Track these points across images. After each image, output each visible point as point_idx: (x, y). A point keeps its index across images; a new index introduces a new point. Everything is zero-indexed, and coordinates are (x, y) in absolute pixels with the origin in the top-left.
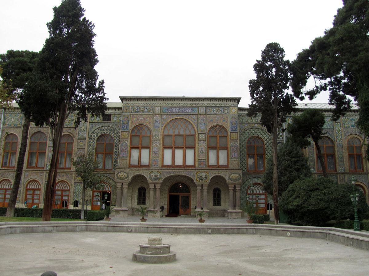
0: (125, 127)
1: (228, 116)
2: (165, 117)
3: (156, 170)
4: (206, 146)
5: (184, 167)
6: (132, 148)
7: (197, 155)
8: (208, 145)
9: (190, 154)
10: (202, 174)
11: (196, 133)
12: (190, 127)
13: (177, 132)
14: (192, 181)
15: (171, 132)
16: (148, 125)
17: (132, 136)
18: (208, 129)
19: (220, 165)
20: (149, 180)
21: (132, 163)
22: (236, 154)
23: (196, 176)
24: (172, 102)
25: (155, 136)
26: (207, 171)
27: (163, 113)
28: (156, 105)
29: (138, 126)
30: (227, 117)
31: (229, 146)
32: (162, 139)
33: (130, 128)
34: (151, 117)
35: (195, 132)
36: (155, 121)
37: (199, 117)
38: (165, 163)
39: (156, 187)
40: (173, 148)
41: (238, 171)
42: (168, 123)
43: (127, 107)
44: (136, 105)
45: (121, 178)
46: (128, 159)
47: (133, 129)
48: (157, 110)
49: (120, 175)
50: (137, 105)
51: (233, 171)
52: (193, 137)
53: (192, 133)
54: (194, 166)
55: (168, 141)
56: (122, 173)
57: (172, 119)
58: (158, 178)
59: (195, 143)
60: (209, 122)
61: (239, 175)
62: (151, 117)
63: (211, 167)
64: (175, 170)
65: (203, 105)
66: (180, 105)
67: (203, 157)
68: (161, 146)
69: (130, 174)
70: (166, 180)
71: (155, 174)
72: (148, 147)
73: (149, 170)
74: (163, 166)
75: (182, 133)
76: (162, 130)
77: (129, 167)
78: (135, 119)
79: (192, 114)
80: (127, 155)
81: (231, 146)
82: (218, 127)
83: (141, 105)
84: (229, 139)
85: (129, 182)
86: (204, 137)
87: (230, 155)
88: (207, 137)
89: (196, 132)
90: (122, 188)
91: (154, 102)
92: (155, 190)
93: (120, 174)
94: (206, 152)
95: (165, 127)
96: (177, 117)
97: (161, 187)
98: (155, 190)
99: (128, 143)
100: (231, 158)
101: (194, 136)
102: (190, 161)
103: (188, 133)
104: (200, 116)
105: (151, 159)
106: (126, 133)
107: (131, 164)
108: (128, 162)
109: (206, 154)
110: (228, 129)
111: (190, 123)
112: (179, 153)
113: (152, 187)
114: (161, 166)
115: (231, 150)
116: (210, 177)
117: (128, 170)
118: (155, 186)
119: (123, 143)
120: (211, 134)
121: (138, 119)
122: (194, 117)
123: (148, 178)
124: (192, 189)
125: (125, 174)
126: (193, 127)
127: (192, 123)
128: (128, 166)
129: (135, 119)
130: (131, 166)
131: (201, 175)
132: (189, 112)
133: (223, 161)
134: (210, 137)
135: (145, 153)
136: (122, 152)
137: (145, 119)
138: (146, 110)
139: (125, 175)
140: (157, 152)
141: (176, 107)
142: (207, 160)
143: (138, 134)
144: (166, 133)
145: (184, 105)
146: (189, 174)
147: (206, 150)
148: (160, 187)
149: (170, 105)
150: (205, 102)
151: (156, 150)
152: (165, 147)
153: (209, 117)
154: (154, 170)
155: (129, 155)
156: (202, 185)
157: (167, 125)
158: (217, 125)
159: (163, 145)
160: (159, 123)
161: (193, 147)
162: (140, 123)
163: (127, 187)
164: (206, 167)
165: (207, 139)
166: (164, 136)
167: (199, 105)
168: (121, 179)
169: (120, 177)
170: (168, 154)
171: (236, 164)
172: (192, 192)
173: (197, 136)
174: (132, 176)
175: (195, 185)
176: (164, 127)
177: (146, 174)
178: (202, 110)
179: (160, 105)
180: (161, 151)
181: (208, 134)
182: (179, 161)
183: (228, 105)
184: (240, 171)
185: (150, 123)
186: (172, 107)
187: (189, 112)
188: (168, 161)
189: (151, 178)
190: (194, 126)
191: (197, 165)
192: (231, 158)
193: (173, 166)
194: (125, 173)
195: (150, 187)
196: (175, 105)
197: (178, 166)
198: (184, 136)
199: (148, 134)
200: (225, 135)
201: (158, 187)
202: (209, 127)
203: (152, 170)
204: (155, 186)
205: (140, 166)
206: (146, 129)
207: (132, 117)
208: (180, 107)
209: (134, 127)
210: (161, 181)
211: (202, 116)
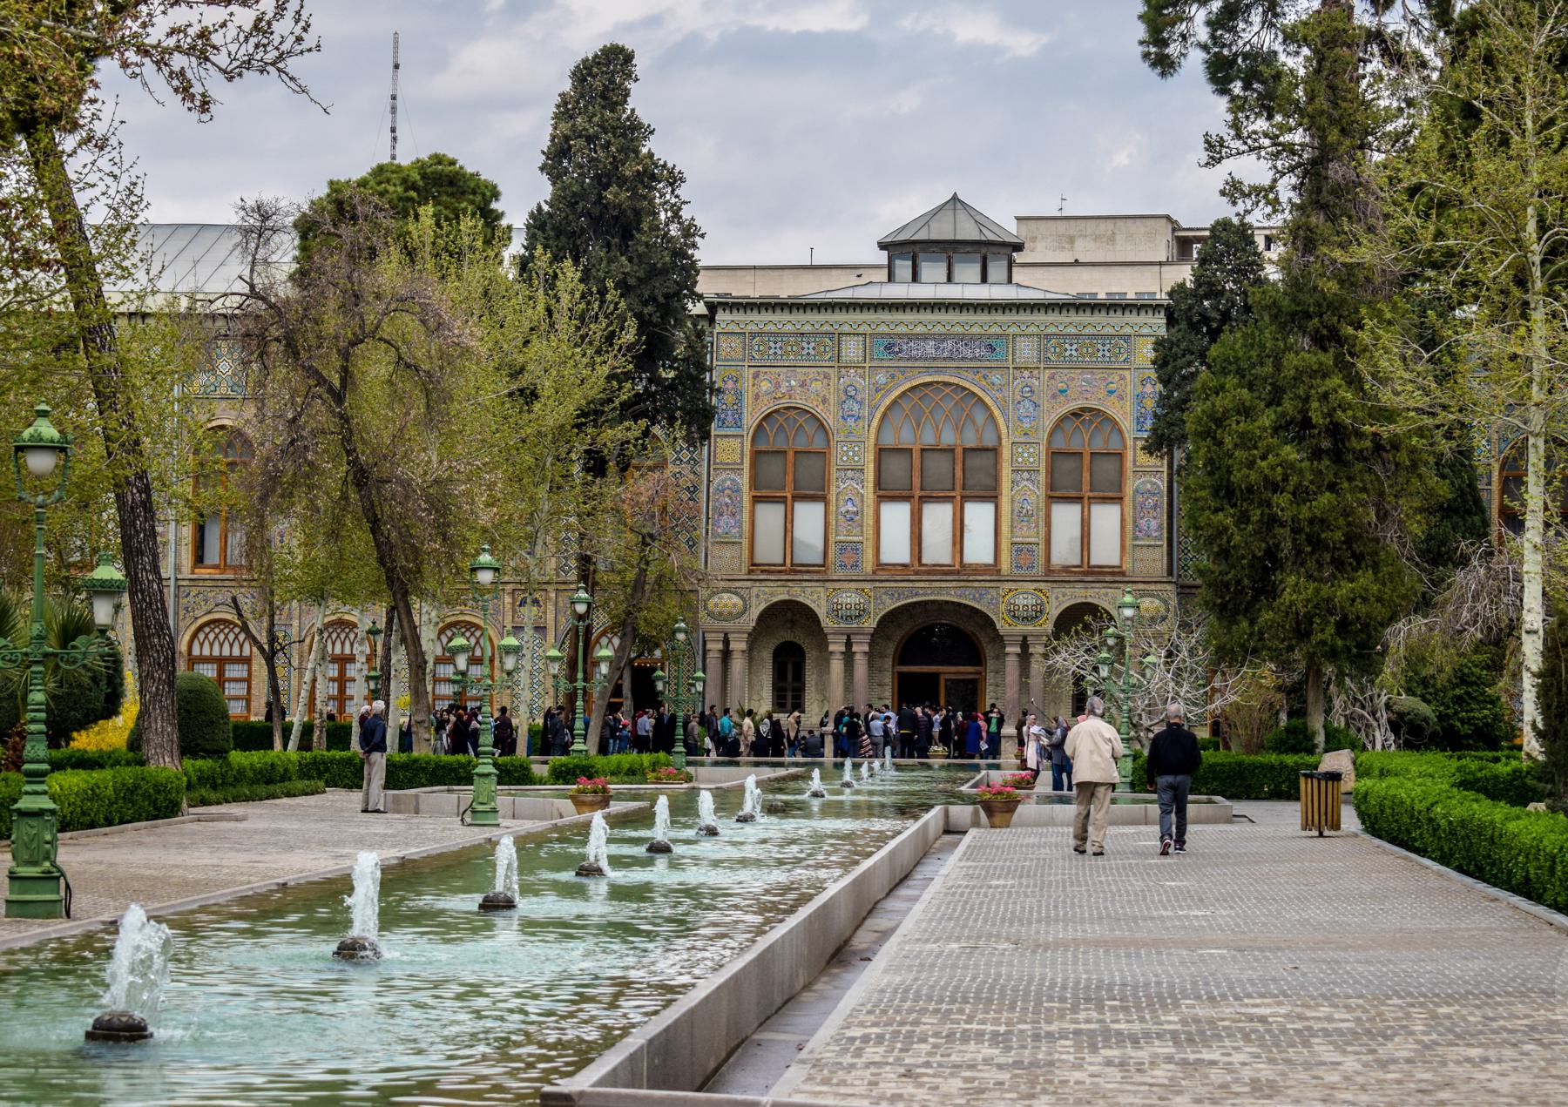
0: (730, 418)
1: (1126, 373)
2: (881, 378)
3: (854, 585)
4: (1042, 493)
5: (958, 573)
6: (757, 500)
7: (1005, 529)
8: (1051, 486)
9: (979, 516)
10: (1024, 601)
11: (1004, 442)
12: (980, 417)
13: (928, 439)
14: (988, 623)
15: (906, 438)
16: (819, 410)
17: (757, 455)
18: (1048, 422)
19: (1094, 562)
20: (827, 623)
21: (761, 557)
22: (1154, 524)
23: (1003, 607)
24: (910, 317)
25: (841, 455)
26: (1042, 586)
27: (875, 364)
28: (846, 329)
29: (776, 411)
30: (1122, 378)
31: (1129, 491)
32: (871, 466)
33: (750, 420)
34: (827, 376)
35: (1000, 439)
36: (846, 391)
37: (1015, 378)
38: (886, 557)
39: (855, 648)
40: (918, 498)
41: (1159, 587)
42: (894, 403)
43: (734, 338)
44: (767, 329)
45: (721, 614)
46: (745, 543)
47: (760, 426)
48: (852, 350)
49: (716, 605)
50: (772, 328)
51: (1141, 586)
52: (991, 454)
53: (989, 441)
54: (993, 569)
55: (895, 466)
56: (725, 596)
57: (908, 385)
58: (861, 613)
59: (996, 478)
60: (1054, 396)
61: (1165, 602)
62: (827, 376)
63: (1055, 576)
64: (922, 584)
65: (1033, 329)
66: (939, 329)
67: (1029, 534)
68: (869, 492)
69: (754, 600)
70: (890, 620)
71: (849, 598)
72: (818, 496)
73: (828, 585)
74: (880, 566)
75: (948, 438)
76: (873, 430)
77: (750, 572)
78: (765, 386)
79: (988, 364)
80: (740, 527)
81: (1136, 491)
82: (1087, 416)
83: (789, 328)
84: (1129, 464)
85: (750, 629)
86: (1037, 457)
87: (1129, 527)
88: (1043, 457)
89: (1004, 436)
90: (726, 654)
91: (840, 317)
92: (848, 656)
93: (715, 600)
94: (1042, 514)
95: (884, 415)
96: (928, 379)
97: (871, 645)
98: (848, 656)
99: (744, 481)
100: (1135, 538)
101: (995, 451)
102: (979, 550)
103: (971, 442)
104: (1017, 373)
105: (832, 538)
106: (735, 443)
107: (759, 559)
108: (746, 553)
109: (1042, 523)
110: (1127, 424)
111: (980, 400)
112: (938, 517)
113: (837, 647)
114: (869, 566)
115: (1134, 508)
116: (1054, 611)
117: (749, 584)
118: (849, 644)
119: (724, 481)
120: (1060, 443)
121: (777, 385)
122: (996, 378)
123: (821, 612)
124: (989, 651)
125: (736, 599)
126: (991, 416)
127: (987, 400)
128: (744, 569)
129: (765, 386)
130: (756, 568)
131: (1021, 601)
132: (974, 359)
133: (1106, 551)
134: (1055, 455)
135: (809, 518)
136: (721, 515)
137: (803, 385)
138: (809, 347)
139: (735, 605)
140: (856, 513)
141: (924, 337)
142: (1042, 546)
143: (780, 444)
144: (889, 441)
145: (958, 329)
146: (974, 599)
147: (1042, 505)
148: (866, 648)
149: (902, 329)
150: (1040, 317)
151: (851, 508)
152: (886, 494)
153: (1052, 377)
154: (846, 585)
155: (746, 526)
156: (1025, 638)
157: (889, 408)
158: (1084, 410)
159: (878, 484)
160: (861, 403)
161: (990, 495)
162: (784, 402)
163: (743, 646)
164: (1039, 570)
165: (1043, 465)
166: (881, 452)
167: (1014, 330)
168: (720, 616)
169: (717, 610)
170: (896, 517)
171: (1154, 561)
172: (991, 665)
173: (1006, 453)
174: (763, 606)
175: (998, 640)
176: (878, 415)
177: (814, 598)
178: (1026, 351)
179: (861, 330)
180: (869, 512)
181: (1049, 442)
182: (937, 550)
183: (1128, 330)
184: (1169, 587)
185: (824, 401)
186: (910, 337)
187: (974, 359)
188: (896, 548)
189: (835, 612)
190: (997, 412)
191: (1005, 566)
192: (1135, 538)
193: (917, 567)
194: (736, 593)
195: (831, 648)
196: (920, 329)
197: (938, 571)
198: (959, 452)
199: (818, 444)
200: (1114, 446)
201: (860, 648)
202: (1054, 417)
203: (837, 585)
204: (849, 644)
205: (793, 570)
206: (810, 428)
207: (756, 376)
208: (941, 338)
209: (765, 418)
210: (871, 624)
211: (1026, 373)
